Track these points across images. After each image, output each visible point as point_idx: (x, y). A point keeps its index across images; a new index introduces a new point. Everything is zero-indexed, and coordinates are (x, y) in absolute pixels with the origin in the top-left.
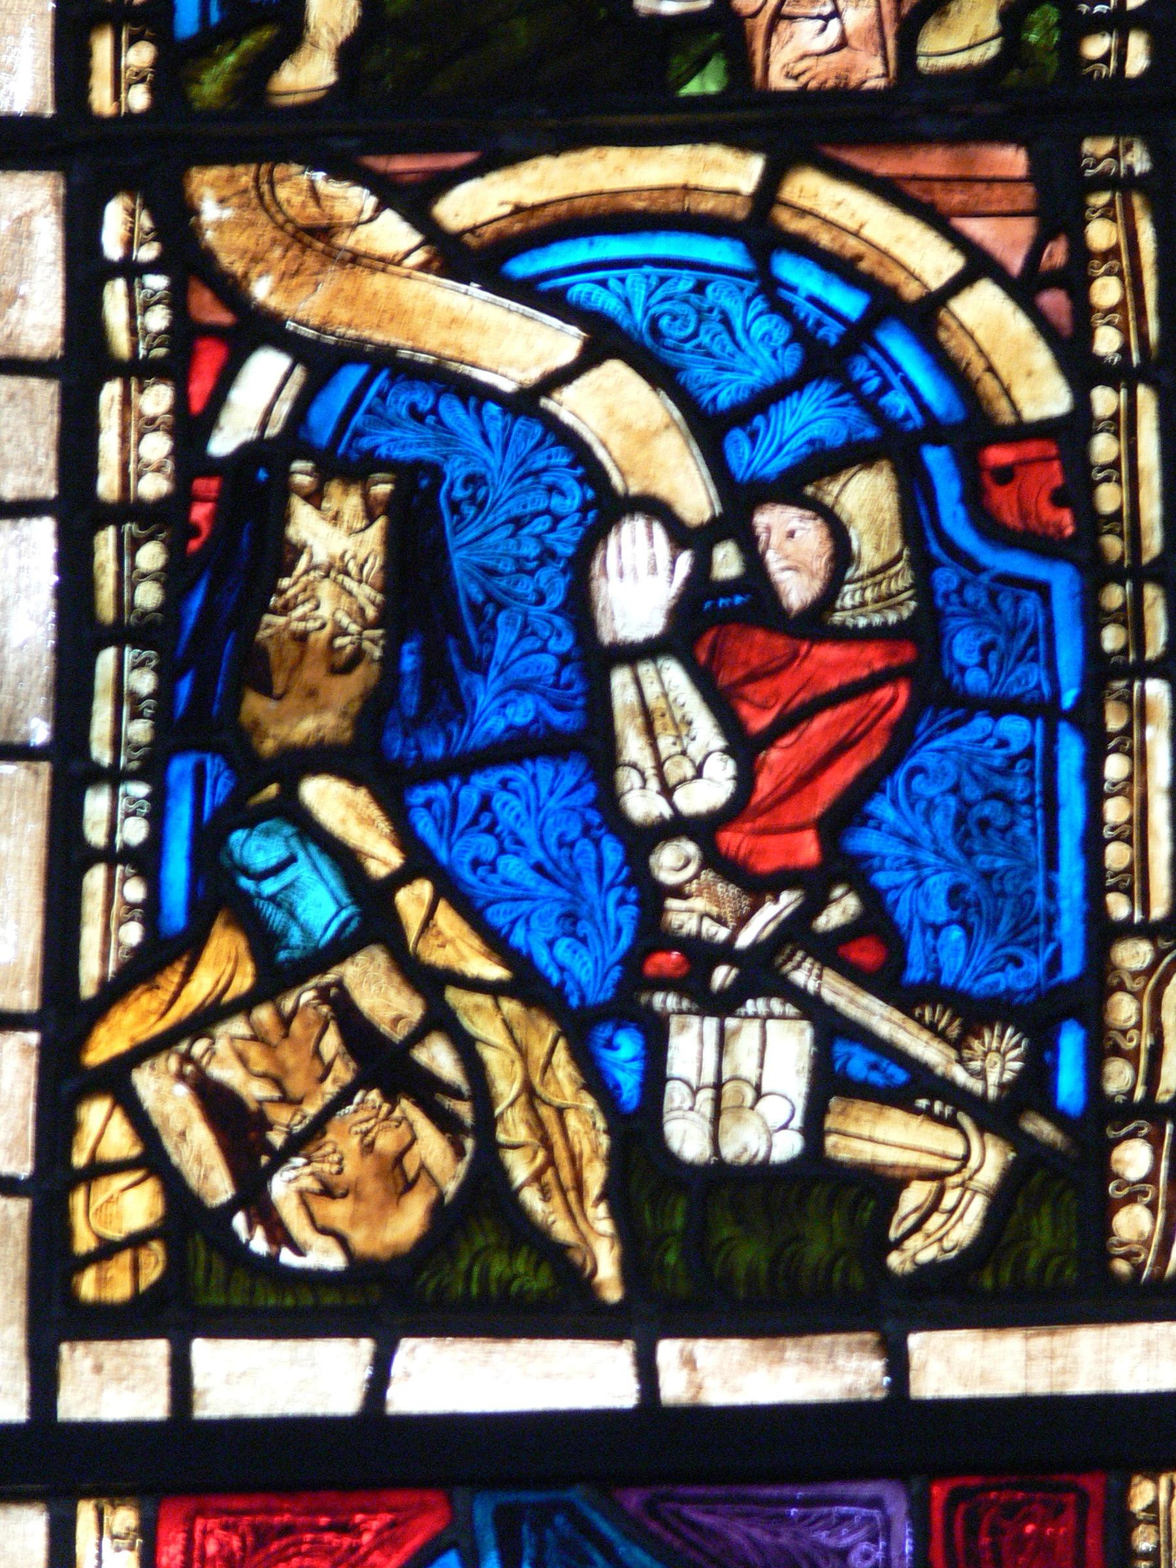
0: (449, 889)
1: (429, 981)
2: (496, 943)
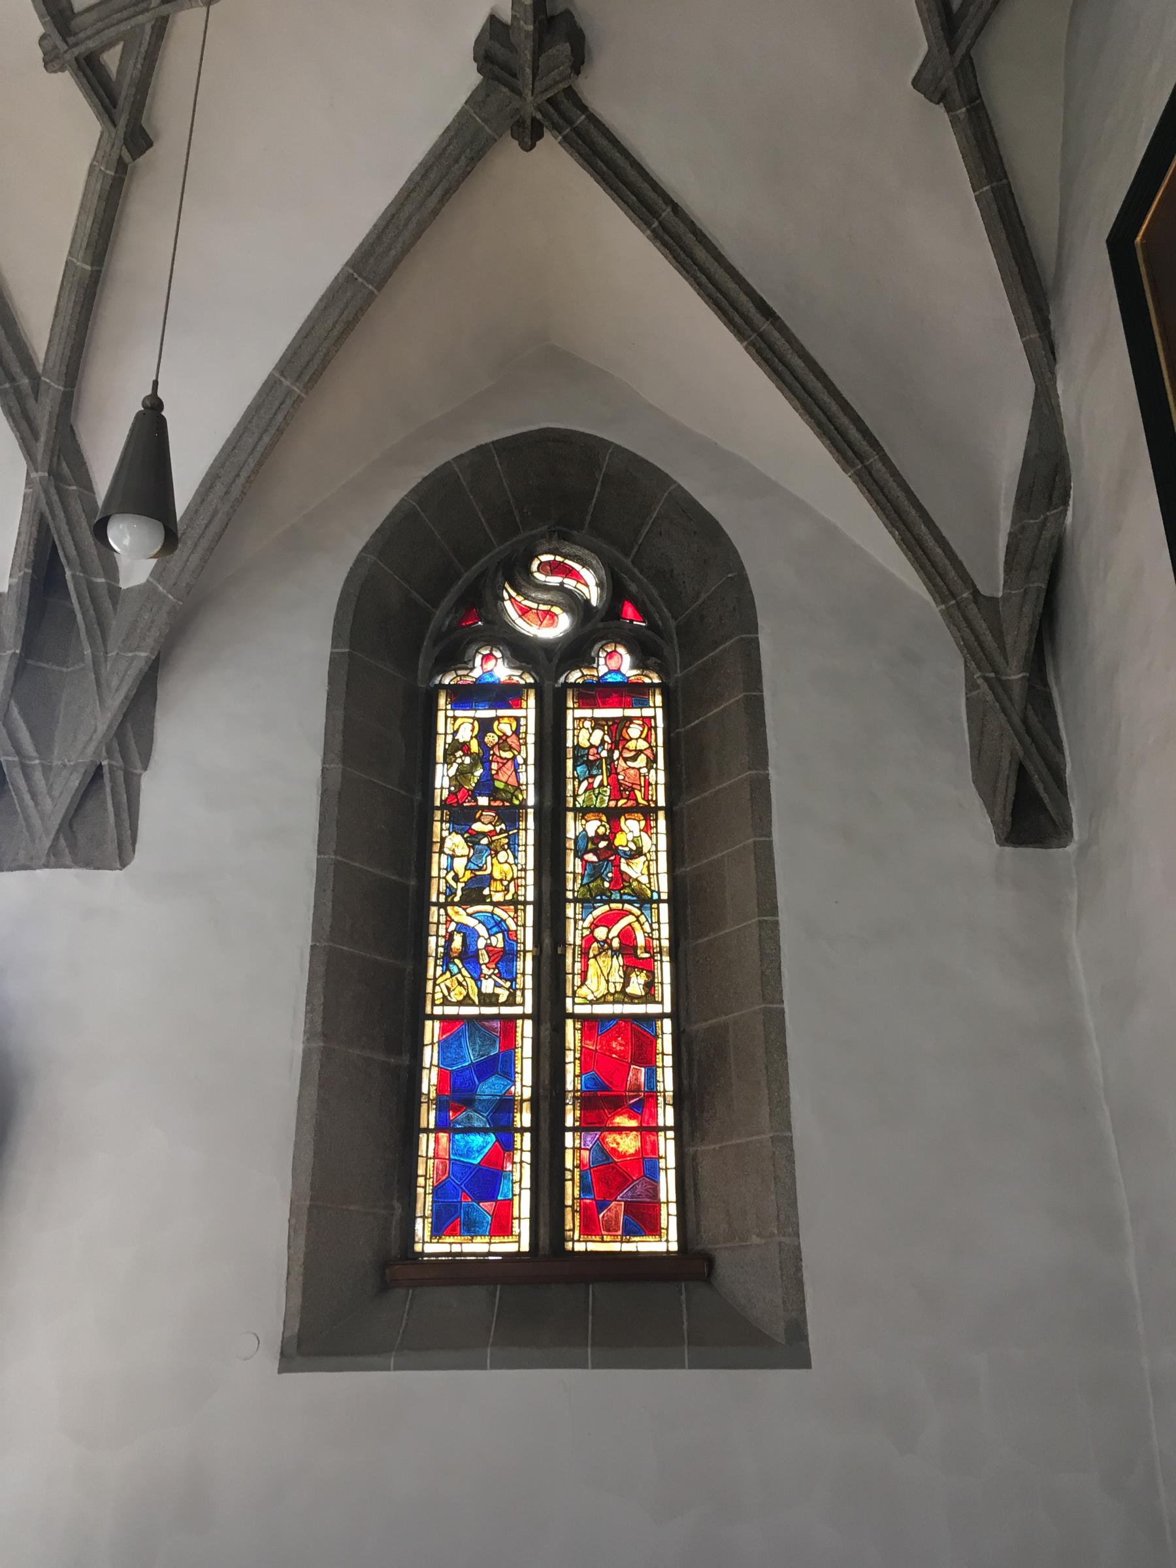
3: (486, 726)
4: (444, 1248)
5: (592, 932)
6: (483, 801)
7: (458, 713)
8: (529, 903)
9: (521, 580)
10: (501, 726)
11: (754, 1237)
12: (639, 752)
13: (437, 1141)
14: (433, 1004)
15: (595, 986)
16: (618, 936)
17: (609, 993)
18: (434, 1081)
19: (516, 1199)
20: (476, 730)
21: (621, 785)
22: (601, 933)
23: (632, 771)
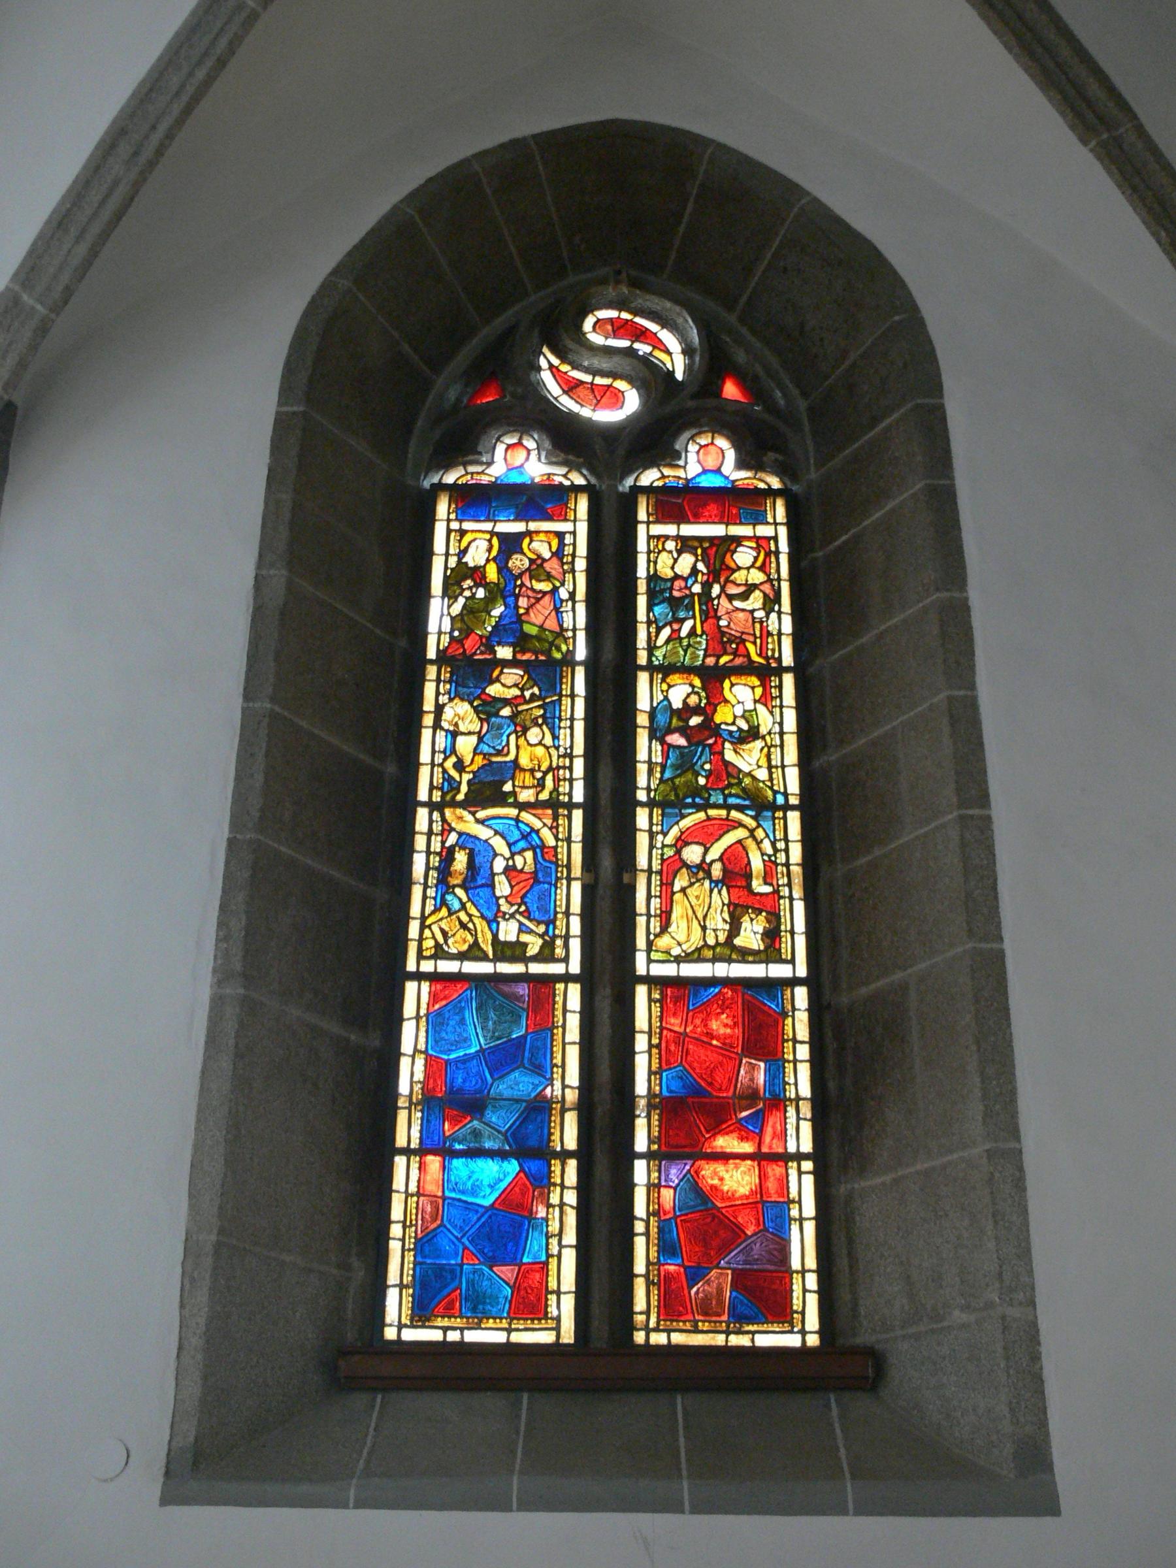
0: (473, 903)
1: (470, 916)
2: (479, 910)
4: (435, 1335)
5: (678, 852)
6: (504, 653)
7: (467, 526)
8: (577, 806)
10: (535, 545)
11: (957, 1313)
12: (751, 588)
13: (422, 1167)
14: (420, 956)
16: (721, 859)
17: (706, 945)
18: (419, 1075)
19: (553, 1263)
20: (496, 535)
21: (723, 634)
22: (692, 854)
23: (741, 615)
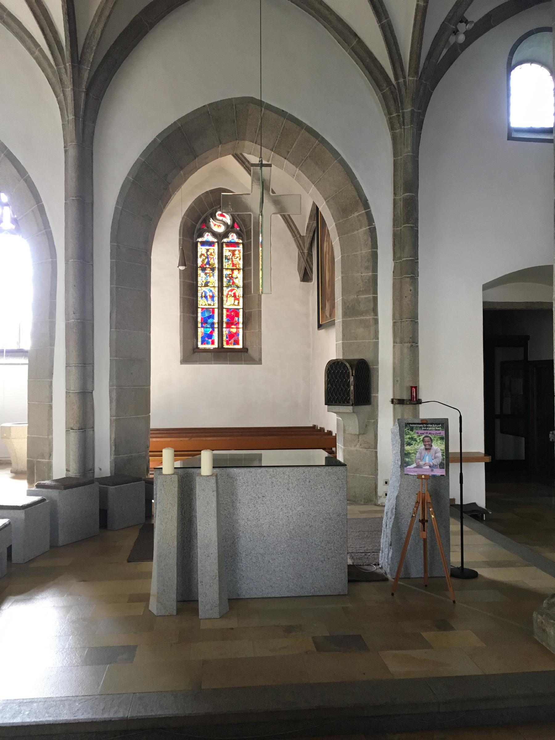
3: (208, 250)
9: (214, 218)
15: (229, 303)
22: (230, 293)
